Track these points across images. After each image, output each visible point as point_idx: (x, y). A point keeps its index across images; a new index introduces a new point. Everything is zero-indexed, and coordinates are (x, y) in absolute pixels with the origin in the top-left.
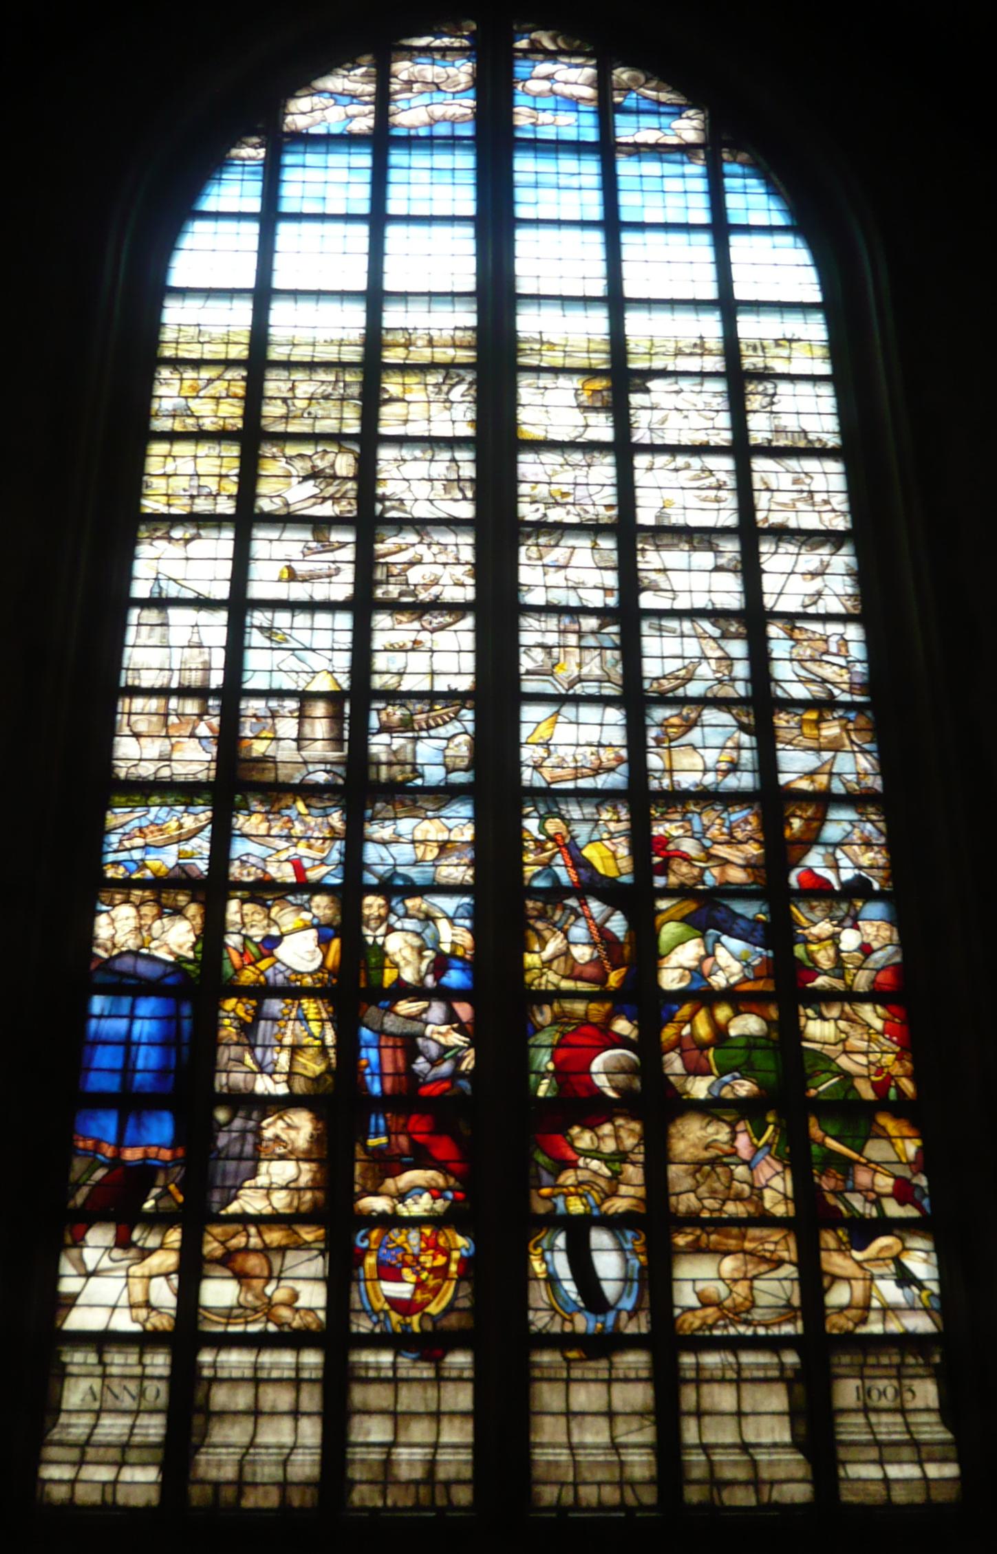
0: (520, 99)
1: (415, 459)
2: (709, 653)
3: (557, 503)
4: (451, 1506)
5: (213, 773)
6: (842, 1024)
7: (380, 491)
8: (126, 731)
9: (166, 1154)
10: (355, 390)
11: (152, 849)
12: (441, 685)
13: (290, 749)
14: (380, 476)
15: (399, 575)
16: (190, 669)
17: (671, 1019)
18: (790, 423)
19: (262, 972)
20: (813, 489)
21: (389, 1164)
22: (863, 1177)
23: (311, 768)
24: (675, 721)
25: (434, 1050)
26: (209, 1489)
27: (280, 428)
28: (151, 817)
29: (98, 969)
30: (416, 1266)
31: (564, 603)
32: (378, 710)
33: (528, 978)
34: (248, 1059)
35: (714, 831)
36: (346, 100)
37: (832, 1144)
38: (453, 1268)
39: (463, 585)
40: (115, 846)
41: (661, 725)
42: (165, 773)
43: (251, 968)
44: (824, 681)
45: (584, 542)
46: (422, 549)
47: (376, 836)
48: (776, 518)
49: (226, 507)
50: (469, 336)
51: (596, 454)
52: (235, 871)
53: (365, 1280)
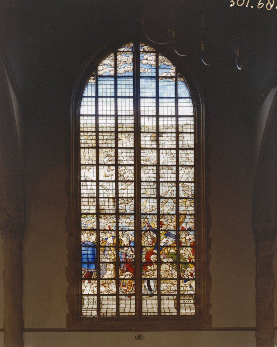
0: (141, 66)
4: (132, 315)
5: (96, 212)
6: (185, 251)
12: (129, 196)
17: (161, 250)
18: (186, 143)
21: (124, 272)
22: (186, 273)
26: (103, 313)
29: (82, 243)
30: (128, 285)
33: (142, 244)
35: (169, 221)
36: (109, 66)
37: (182, 268)
38: (132, 285)
39: (132, 177)
42: (89, 212)
44: (187, 194)
46: (126, 170)
47: (120, 222)
49: (94, 162)
50: (132, 125)
51: (153, 150)
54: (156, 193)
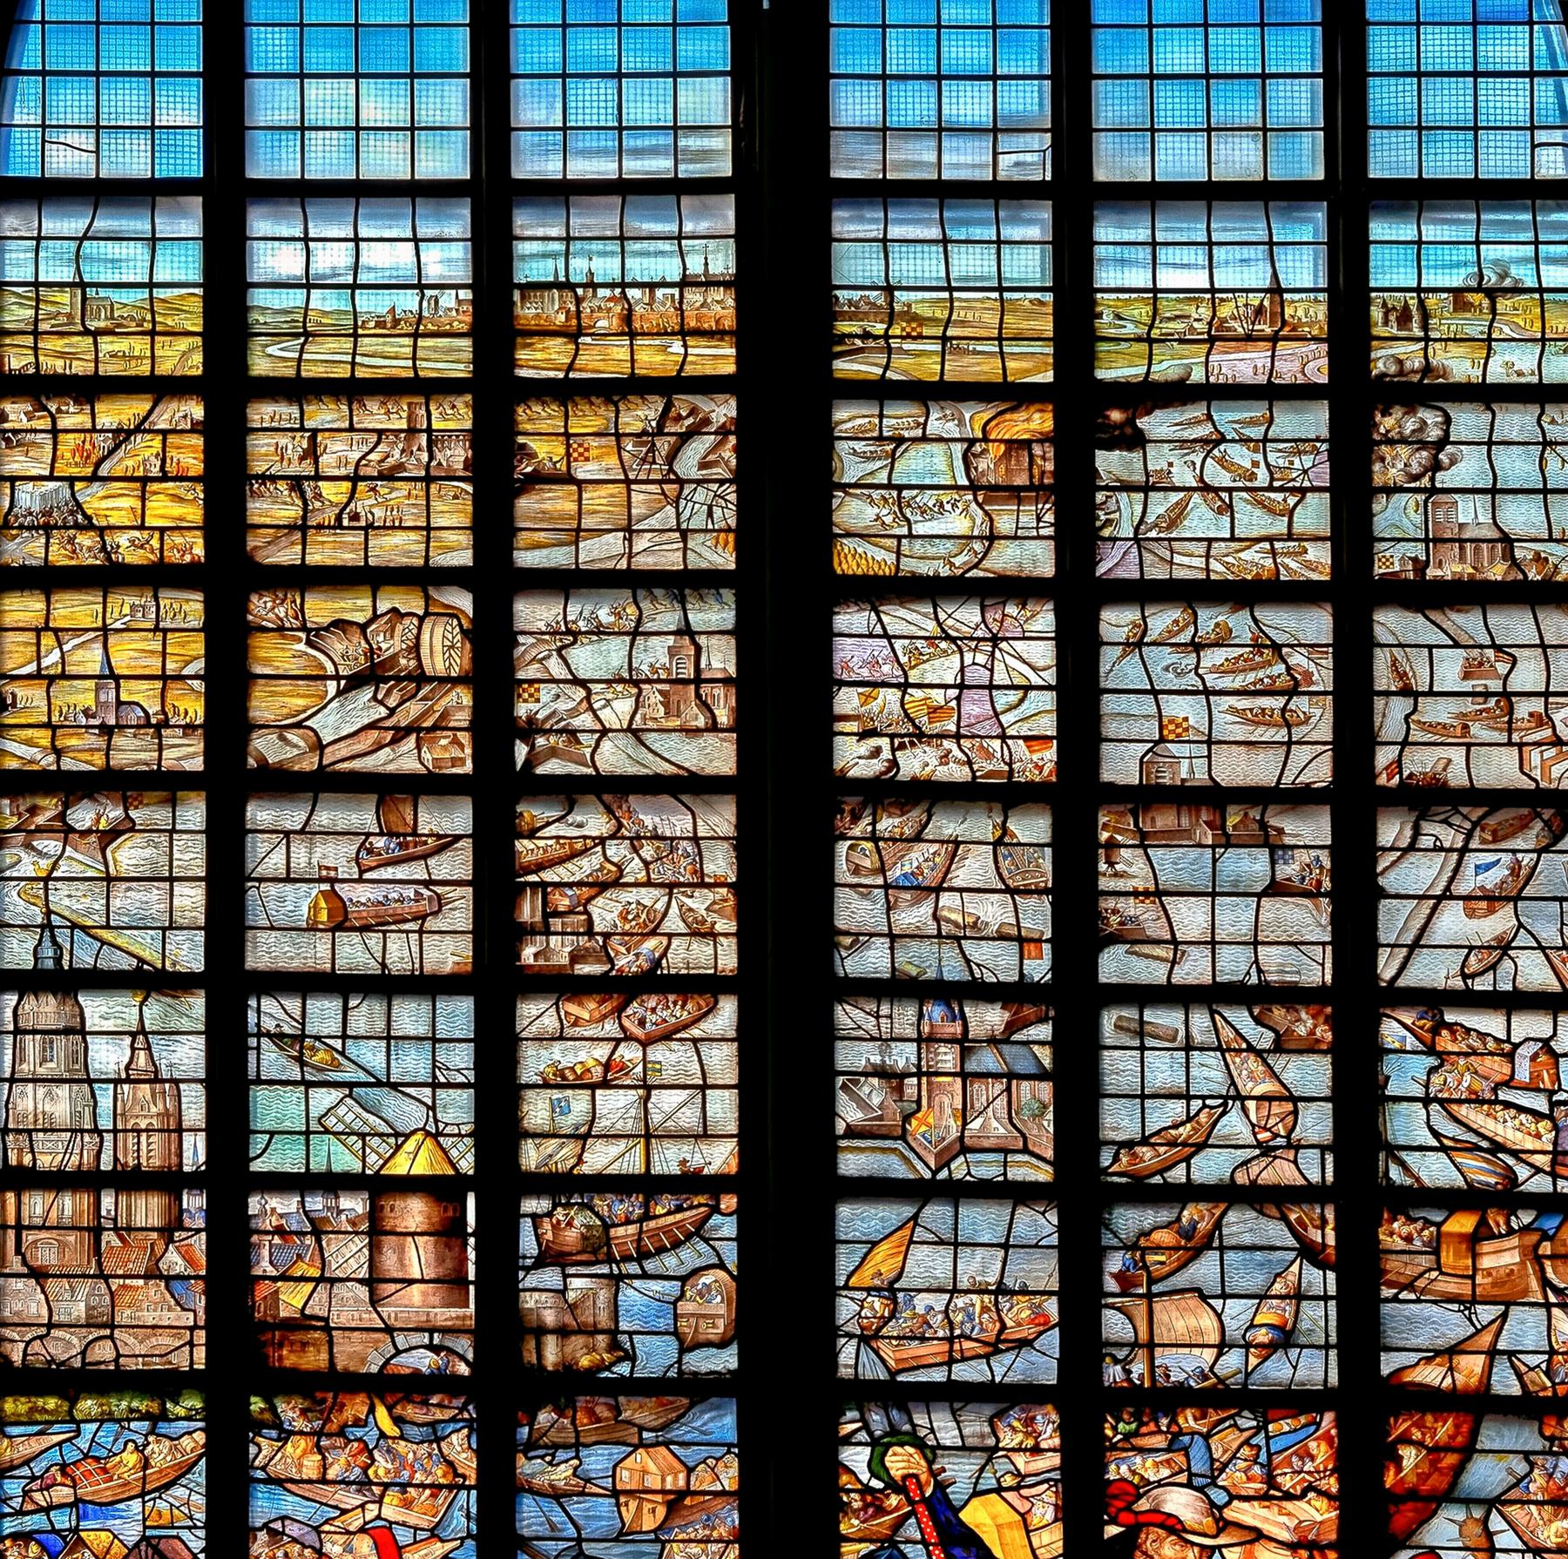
1: (600, 631)
2: (1246, 1087)
3: (920, 736)
5: (200, 1354)
7: (522, 710)
8: (15, 1264)
10: (456, 455)
12: (669, 1159)
13: (357, 1300)
14: (521, 675)
15: (571, 912)
16: (139, 1131)
18: (1470, 513)
20: (1515, 684)
23: (401, 1340)
24: (1164, 1237)
27: (286, 555)
28: (83, 1444)
31: (931, 974)
32: (536, 1218)
39: (712, 935)
40: (16, 1503)
41: (1133, 1247)
44: (1497, 1147)
45: (980, 825)
46: (617, 851)
48: (1420, 762)
50: (721, 307)
51: (1012, 610)
54: (1043, 1134)
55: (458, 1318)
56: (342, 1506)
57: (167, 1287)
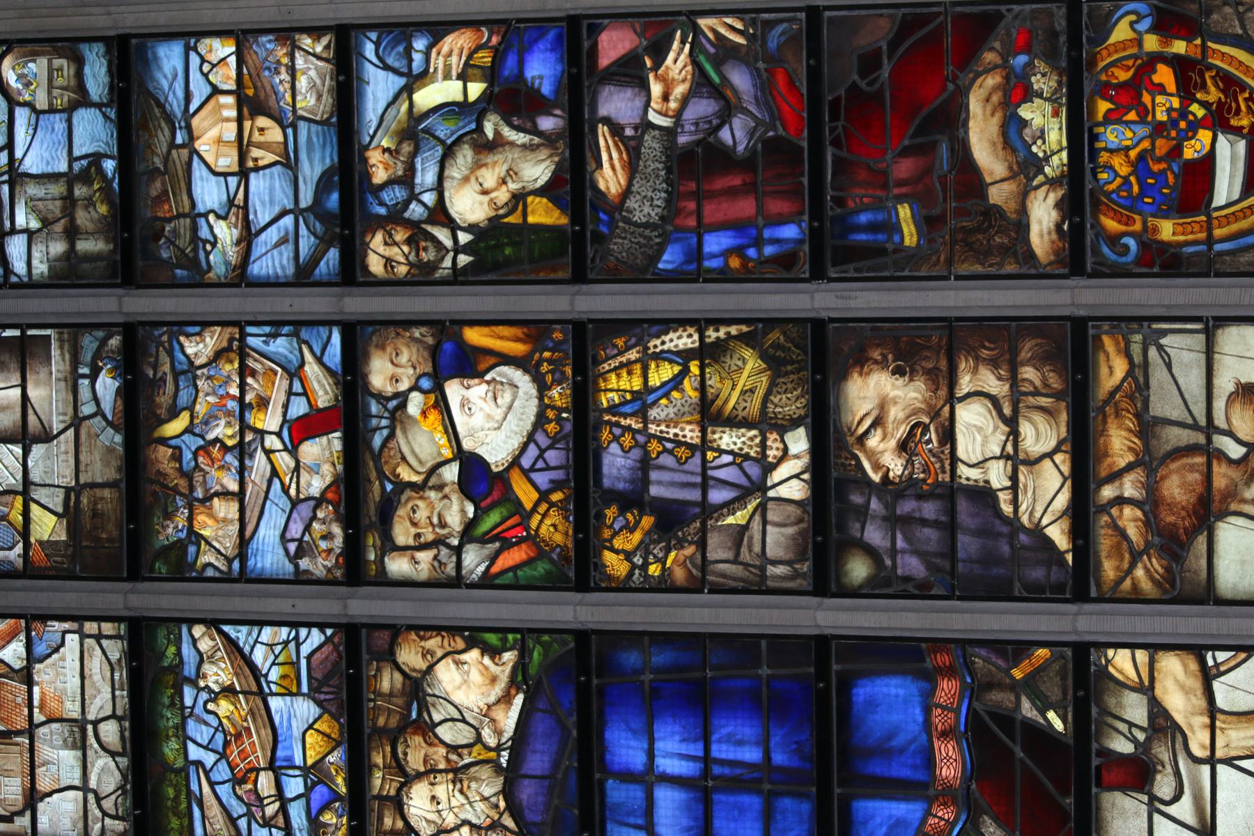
5: (108, 628)
8: (23, 822)
9: (947, 689)
11: (280, 753)
13: (47, 457)
19: (544, 496)
23: (87, 409)
25: (703, 108)
28: (209, 759)
34: (738, 518)
38: (1179, 47)
42: (110, 731)
43: (534, 523)
47: (233, 254)
52: (317, 566)
53: (1210, 241)
55: (61, 348)
56: (268, 474)
57: (41, 661)
